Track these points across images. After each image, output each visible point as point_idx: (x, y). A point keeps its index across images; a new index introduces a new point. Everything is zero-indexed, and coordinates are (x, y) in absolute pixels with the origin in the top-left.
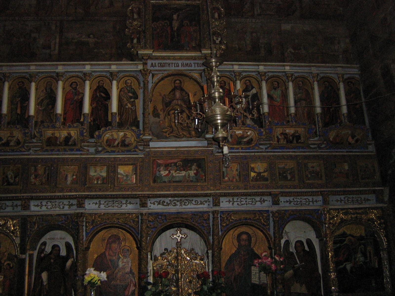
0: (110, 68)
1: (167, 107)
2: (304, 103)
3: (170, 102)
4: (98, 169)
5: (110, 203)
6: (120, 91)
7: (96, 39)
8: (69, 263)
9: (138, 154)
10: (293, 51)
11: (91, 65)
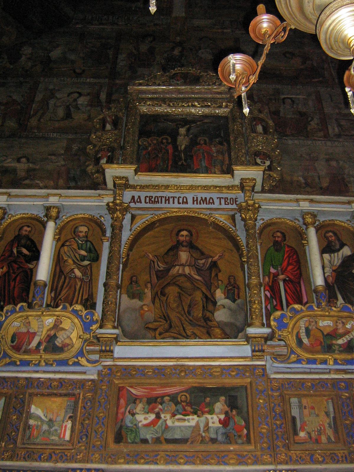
0: (47, 201)
6: (63, 245)
7: (31, 165)
9: (85, 373)
11: (9, 195)
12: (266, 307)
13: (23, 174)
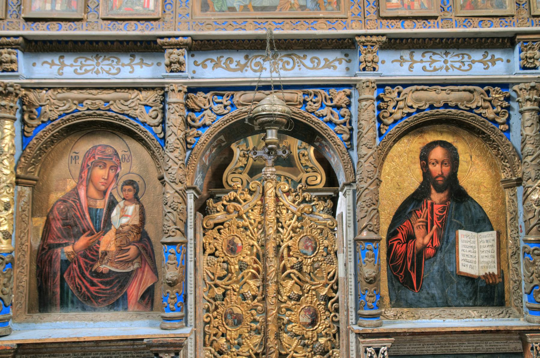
5: (89, 62)
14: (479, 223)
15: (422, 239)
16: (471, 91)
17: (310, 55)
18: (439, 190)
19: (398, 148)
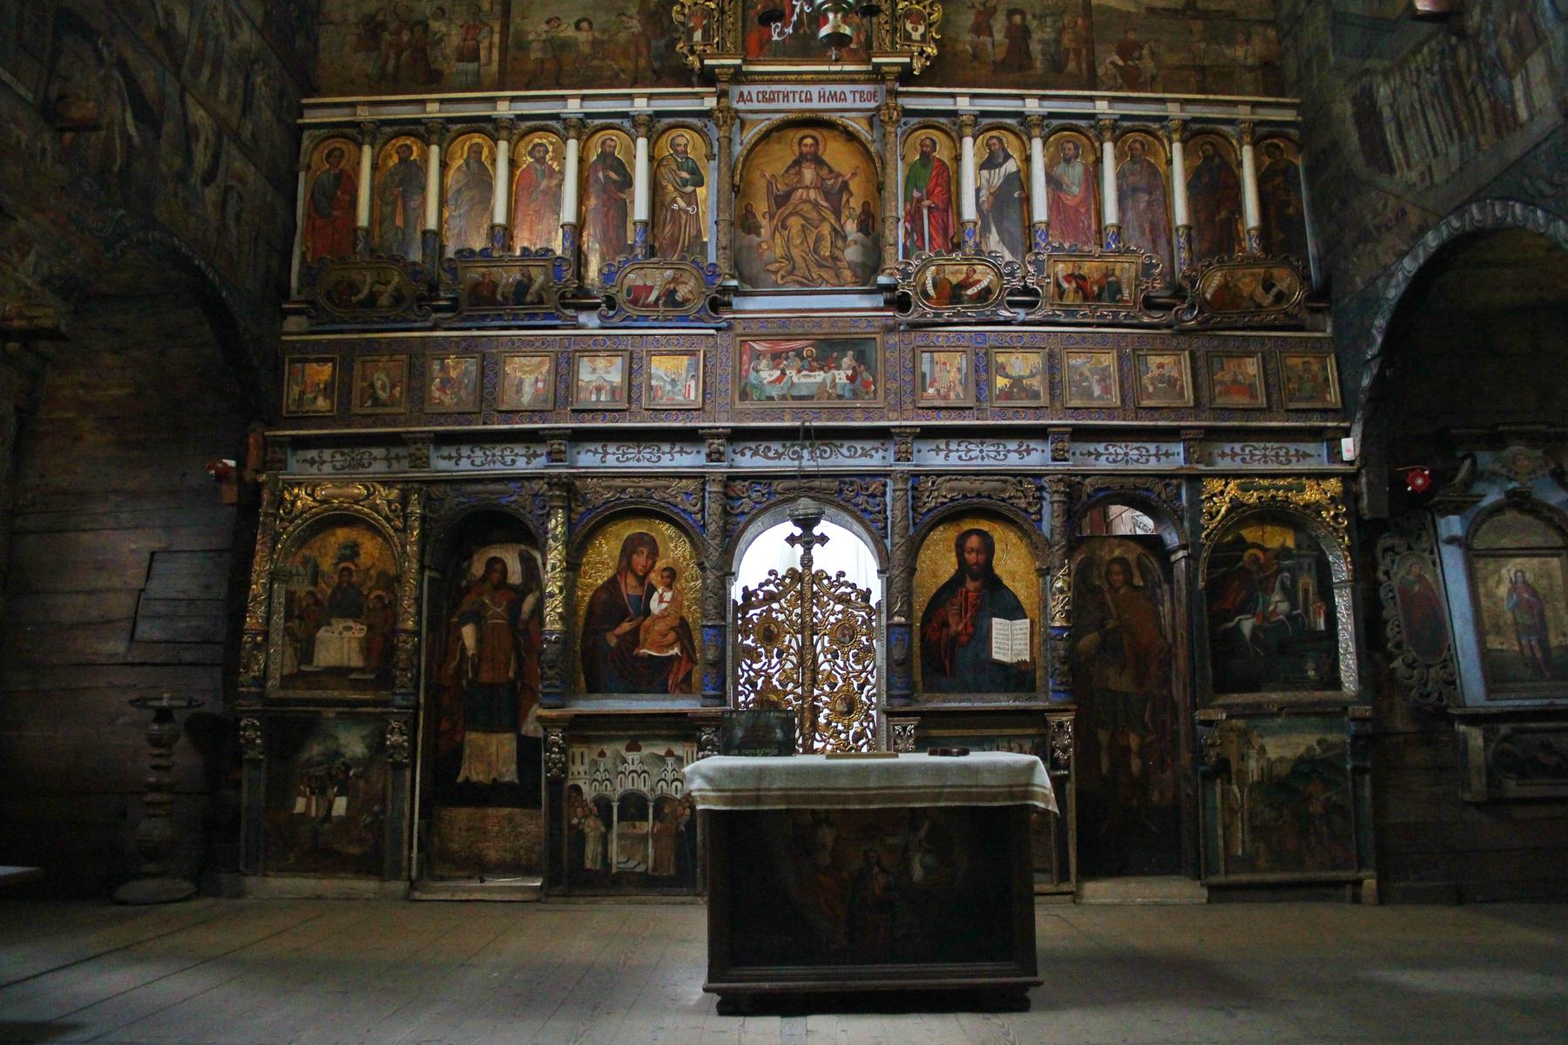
1: (778, 207)
2: (1144, 197)
3: (788, 195)
4: (601, 363)
8: (529, 603)
10: (1121, 63)
12: (905, 245)
13: (586, 49)
14: (1013, 610)
15: (956, 626)
16: (1005, 482)
17: (847, 444)
18: (974, 579)
19: (935, 535)
